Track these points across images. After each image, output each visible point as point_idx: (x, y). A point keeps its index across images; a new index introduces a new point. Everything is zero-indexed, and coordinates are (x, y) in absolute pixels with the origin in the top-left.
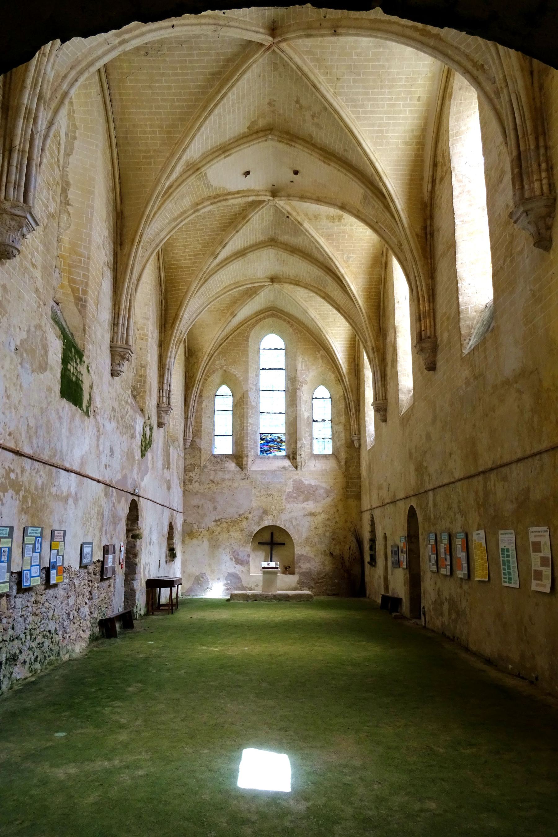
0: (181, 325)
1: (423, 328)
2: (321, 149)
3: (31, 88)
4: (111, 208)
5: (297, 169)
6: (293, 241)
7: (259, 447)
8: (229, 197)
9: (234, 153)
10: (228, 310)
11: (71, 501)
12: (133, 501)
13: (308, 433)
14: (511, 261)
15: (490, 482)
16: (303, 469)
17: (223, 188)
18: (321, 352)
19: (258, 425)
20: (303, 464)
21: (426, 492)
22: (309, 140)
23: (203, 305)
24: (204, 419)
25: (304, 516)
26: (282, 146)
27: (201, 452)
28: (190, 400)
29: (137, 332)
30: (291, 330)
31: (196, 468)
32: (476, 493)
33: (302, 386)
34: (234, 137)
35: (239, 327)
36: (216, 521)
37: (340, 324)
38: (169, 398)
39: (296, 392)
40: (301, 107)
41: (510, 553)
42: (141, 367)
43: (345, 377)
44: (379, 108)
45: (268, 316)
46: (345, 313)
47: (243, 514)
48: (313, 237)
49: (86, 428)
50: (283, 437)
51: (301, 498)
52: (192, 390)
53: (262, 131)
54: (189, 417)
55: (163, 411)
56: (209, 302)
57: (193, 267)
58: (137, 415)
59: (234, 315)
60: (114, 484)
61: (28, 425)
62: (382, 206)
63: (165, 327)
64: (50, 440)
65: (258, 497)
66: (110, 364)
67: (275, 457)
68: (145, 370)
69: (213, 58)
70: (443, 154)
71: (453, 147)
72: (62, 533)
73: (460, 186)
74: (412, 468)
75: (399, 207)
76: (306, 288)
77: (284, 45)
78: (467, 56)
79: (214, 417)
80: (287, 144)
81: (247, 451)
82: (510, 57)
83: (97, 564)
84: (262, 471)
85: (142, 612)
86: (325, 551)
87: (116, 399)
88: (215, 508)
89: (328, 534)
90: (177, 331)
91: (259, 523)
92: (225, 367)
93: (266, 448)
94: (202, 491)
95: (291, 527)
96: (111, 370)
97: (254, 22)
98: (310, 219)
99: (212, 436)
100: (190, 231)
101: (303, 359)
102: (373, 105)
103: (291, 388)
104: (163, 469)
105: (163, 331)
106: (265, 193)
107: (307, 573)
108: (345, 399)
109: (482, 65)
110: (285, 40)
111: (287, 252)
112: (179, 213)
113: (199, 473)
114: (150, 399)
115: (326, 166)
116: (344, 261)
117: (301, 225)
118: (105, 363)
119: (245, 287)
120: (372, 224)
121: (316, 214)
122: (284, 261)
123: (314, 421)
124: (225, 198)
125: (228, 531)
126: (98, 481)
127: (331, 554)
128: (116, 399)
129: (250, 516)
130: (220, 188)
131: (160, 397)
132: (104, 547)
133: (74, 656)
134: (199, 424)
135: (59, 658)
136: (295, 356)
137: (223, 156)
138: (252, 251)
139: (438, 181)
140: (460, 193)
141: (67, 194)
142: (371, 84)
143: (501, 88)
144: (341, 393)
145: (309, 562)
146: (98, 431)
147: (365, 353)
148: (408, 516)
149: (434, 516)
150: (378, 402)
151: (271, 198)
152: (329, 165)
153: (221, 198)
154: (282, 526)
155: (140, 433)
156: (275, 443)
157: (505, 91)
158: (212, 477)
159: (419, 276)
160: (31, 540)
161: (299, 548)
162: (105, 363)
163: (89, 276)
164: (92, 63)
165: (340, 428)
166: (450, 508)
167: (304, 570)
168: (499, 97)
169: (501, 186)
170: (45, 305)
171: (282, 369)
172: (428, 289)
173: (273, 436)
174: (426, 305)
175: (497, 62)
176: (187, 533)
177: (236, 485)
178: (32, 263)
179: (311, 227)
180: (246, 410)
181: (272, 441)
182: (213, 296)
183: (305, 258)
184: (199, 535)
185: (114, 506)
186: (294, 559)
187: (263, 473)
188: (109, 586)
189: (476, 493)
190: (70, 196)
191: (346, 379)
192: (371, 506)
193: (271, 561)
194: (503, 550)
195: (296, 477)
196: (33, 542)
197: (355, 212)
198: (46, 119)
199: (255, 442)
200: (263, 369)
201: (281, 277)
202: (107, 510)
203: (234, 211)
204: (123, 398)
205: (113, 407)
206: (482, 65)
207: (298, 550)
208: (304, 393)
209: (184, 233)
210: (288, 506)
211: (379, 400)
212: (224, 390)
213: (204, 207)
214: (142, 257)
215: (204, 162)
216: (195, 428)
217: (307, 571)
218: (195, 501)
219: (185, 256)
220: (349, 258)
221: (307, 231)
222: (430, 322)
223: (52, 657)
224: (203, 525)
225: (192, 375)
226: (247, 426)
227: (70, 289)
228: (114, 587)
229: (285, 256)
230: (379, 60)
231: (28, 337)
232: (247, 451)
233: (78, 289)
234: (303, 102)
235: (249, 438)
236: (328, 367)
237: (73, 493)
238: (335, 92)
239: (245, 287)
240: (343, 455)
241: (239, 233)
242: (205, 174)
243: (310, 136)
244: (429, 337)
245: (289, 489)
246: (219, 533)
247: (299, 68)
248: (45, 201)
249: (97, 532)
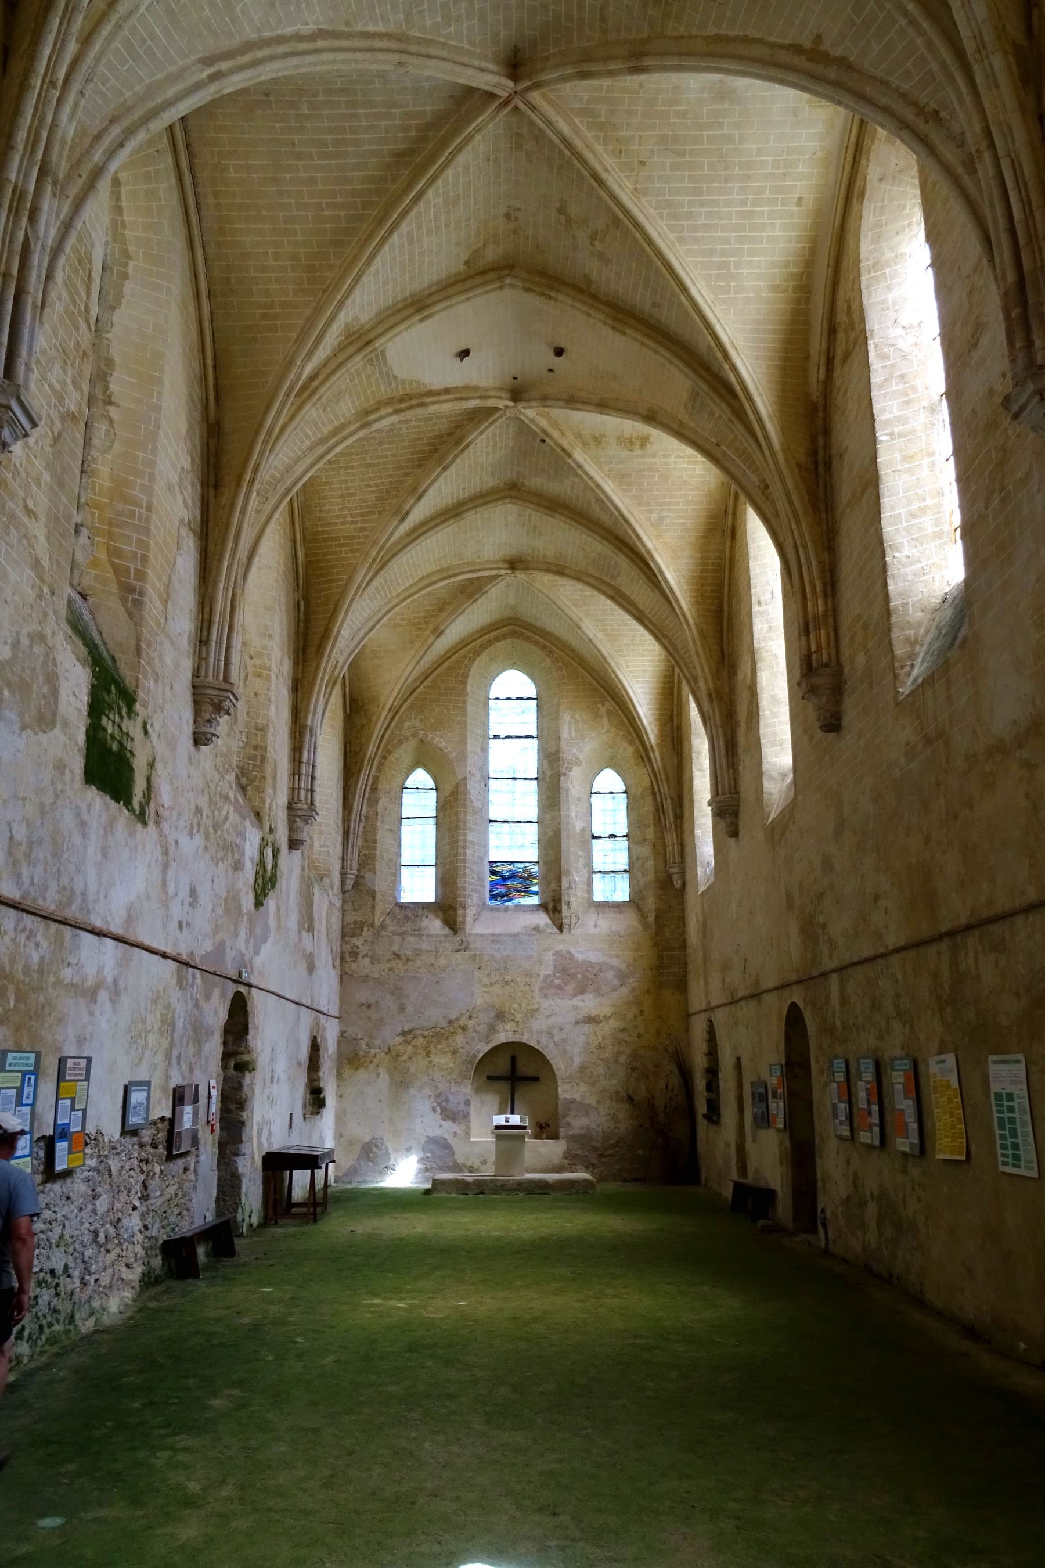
0: (336, 649)
1: (813, 648)
2: (608, 304)
3: (25, 149)
4: (197, 416)
5: (562, 346)
6: (554, 487)
7: (488, 888)
8: (428, 400)
9: (440, 311)
10: (427, 623)
11: (103, 996)
12: (238, 995)
13: (582, 861)
14: (1002, 500)
15: (966, 955)
16: (573, 931)
17: (418, 383)
18: (607, 703)
19: (485, 846)
20: (574, 921)
21: (824, 975)
22: (584, 287)
23: (378, 611)
24: (382, 835)
25: (577, 1023)
26: (532, 300)
27: (374, 898)
28: (354, 797)
29: (249, 662)
30: (548, 660)
31: (365, 929)
33: (570, 770)
34: (439, 282)
35: (449, 658)
36: (404, 1033)
37: (644, 650)
38: (312, 791)
39: (559, 780)
40: (569, 221)
41: (1014, 1104)
42: (257, 730)
43: (653, 751)
44: (721, 219)
45: (504, 636)
46: (654, 625)
47: (457, 1019)
48: (591, 478)
49: (140, 848)
50: (535, 869)
51: (570, 988)
52: (358, 780)
53: (493, 269)
54: (352, 830)
55: (299, 816)
56: (390, 606)
57: (358, 537)
58: (247, 823)
59: (438, 633)
60: (197, 961)
61: (11, 838)
62: (728, 411)
63: (304, 652)
64: (59, 870)
65: (486, 986)
66: (191, 721)
67: (519, 908)
68: (265, 736)
69: (398, 122)
70: (849, 307)
71: (869, 292)
72: (83, 1063)
73: (885, 366)
74: (794, 929)
75: (763, 411)
76: (579, 580)
77: (535, 96)
78: (904, 96)
79: (400, 829)
80: (542, 294)
81: (464, 897)
82: (998, 87)
83: (160, 1125)
84: (493, 935)
85: (255, 1220)
86: (617, 1092)
87: (203, 791)
88: (402, 1009)
89: (623, 1059)
90: (328, 661)
91: (487, 1036)
92: (422, 732)
93: (501, 890)
94: (376, 975)
95: (551, 1045)
96: (195, 733)
97: (478, 51)
98: (585, 444)
99: (395, 867)
100: (353, 467)
101: (572, 717)
102: (709, 215)
103: (548, 774)
104: (300, 932)
105: (301, 660)
106: (498, 394)
107: (583, 1136)
108: (654, 794)
109: (936, 112)
110: (537, 86)
111: (542, 509)
112: (330, 428)
113: (370, 940)
114: (275, 793)
115: (618, 336)
116: (652, 525)
117: (569, 455)
118: (180, 719)
119: (460, 578)
120: (707, 447)
121: (597, 434)
122: (535, 528)
123: (594, 837)
124: (420, 401)
125: (428, 1055)
126: (164, 956)
127: (630, 1098)
128: (203, 791)
129: (471, 1024)
130: (411, 383)
131: (293, 789)
132: (175, 1090)
133: (106, 1320)
134: (371, 843)
135: (72, 1327)
136: (558, 712)
137: (417, 317)
138: (474, 507)
139: (838, 360)
140: (885, 380)
141: (108, 382)
142: (705, 172)
143: (978, 151)
144: (646, 783)
145: (587, 1114)
146: (166, 853)
147: (693, 706)
148: (786, 1025)
149: (843, 1023)
150: (721, 798)
151: (511, 404)
152: (624, 333)
153: (414, 402)
154: (532, 1044)
155: (252, 859)
156: (519, 880)
157: (987, 156)
158: (395, 948)
159: (805, 546)
160: (14, 1080)
161: (567, 1087)
162: (180, 719)
163: (148, 544)
164: (153, 114)
165: (646, 851)
166: (876, 1006)
167: (576, 1131)
168: (972, 170)
169: (976, 355)
170: (53, 593)
171: (531, 737)
172: (822, 571)
173: (514, 867)
174: (820, 602)
175: (968, 100)
176: (348, 1059)
177: (443, 962)
178: (26, 507)
179: (589, 460)
180: (462, 815)
181: (513, 876)
182: (398, 595)
183: (576, 521)
184: (371, 1062)
185: (196, 1005)
186: (556, 1110)
187: (496, 939)
188: (186, 1169)
190: (113, 387)
191: (656, 756)
192: (709, 1003)
193: (512, 1113)
194: (998, 1096)
195: (560, 947)
196: (18, 1084)
197: (675, 426)
198: (58, 215)
199: (480, 879)
200: (496, 737)
201: (529, 559)
202: (182, 1014)
203: (439, 430)
204: (219, 789)
205: (197, 807)
206: (936, 112)
207: (565, 1092)
208: (573, 783)
209: (342, 472)
210: (545, 1004)
211: (724, 794)
212: (420, 777)
213: (381, 418)
214: (257, 512)
215: (380, 329)
216: (363, 852)
217: (584, 1132)
218: (363, 995)
219: (345, 517)
220: (661, 518)
221: (580, 466)
222: (828, 634)
223: (57, 1327)
224: (377, 1042)
225: (357, 749)
226: (464, 847)
227: (111, 570)
228: (195, 1171)
229: (535, 516)
230: (721, 125)
231: (15, 656)
232: (464, 897)
233: (128, 569)
234: (573, 211)
235: (467, 871)
236: (621, 733)
237: (110, 979)
238: (636, 189)
239: (460, 578)
240: (651, 904)
241: (447, 473)
242: (383, 352)
243: (587, 278)
244: (827, 665)
245: (547, 970)
246: (410, 1058)
247: (565, 141)
248: (58, 387)
249: (159, 1059)
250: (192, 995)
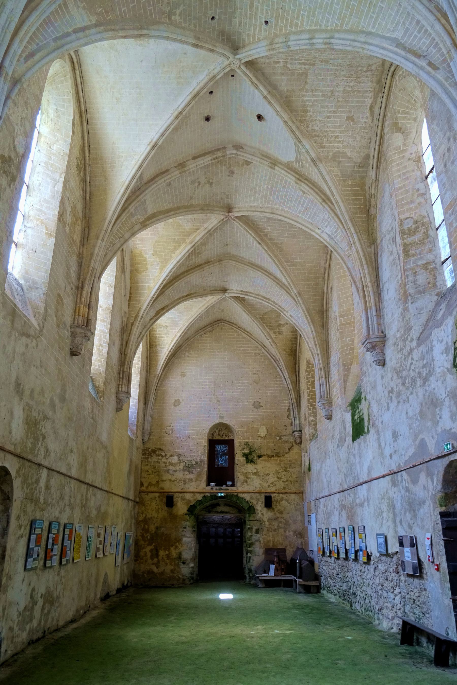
11: (366, 504)
32: (82, 495)
126: (384, 476)
149: (44, 499)
166: (62, 497)
185: (408, 490)
189: (82, 495)
202: (399, 498)
249: (390, 523)
250: (403, 487)
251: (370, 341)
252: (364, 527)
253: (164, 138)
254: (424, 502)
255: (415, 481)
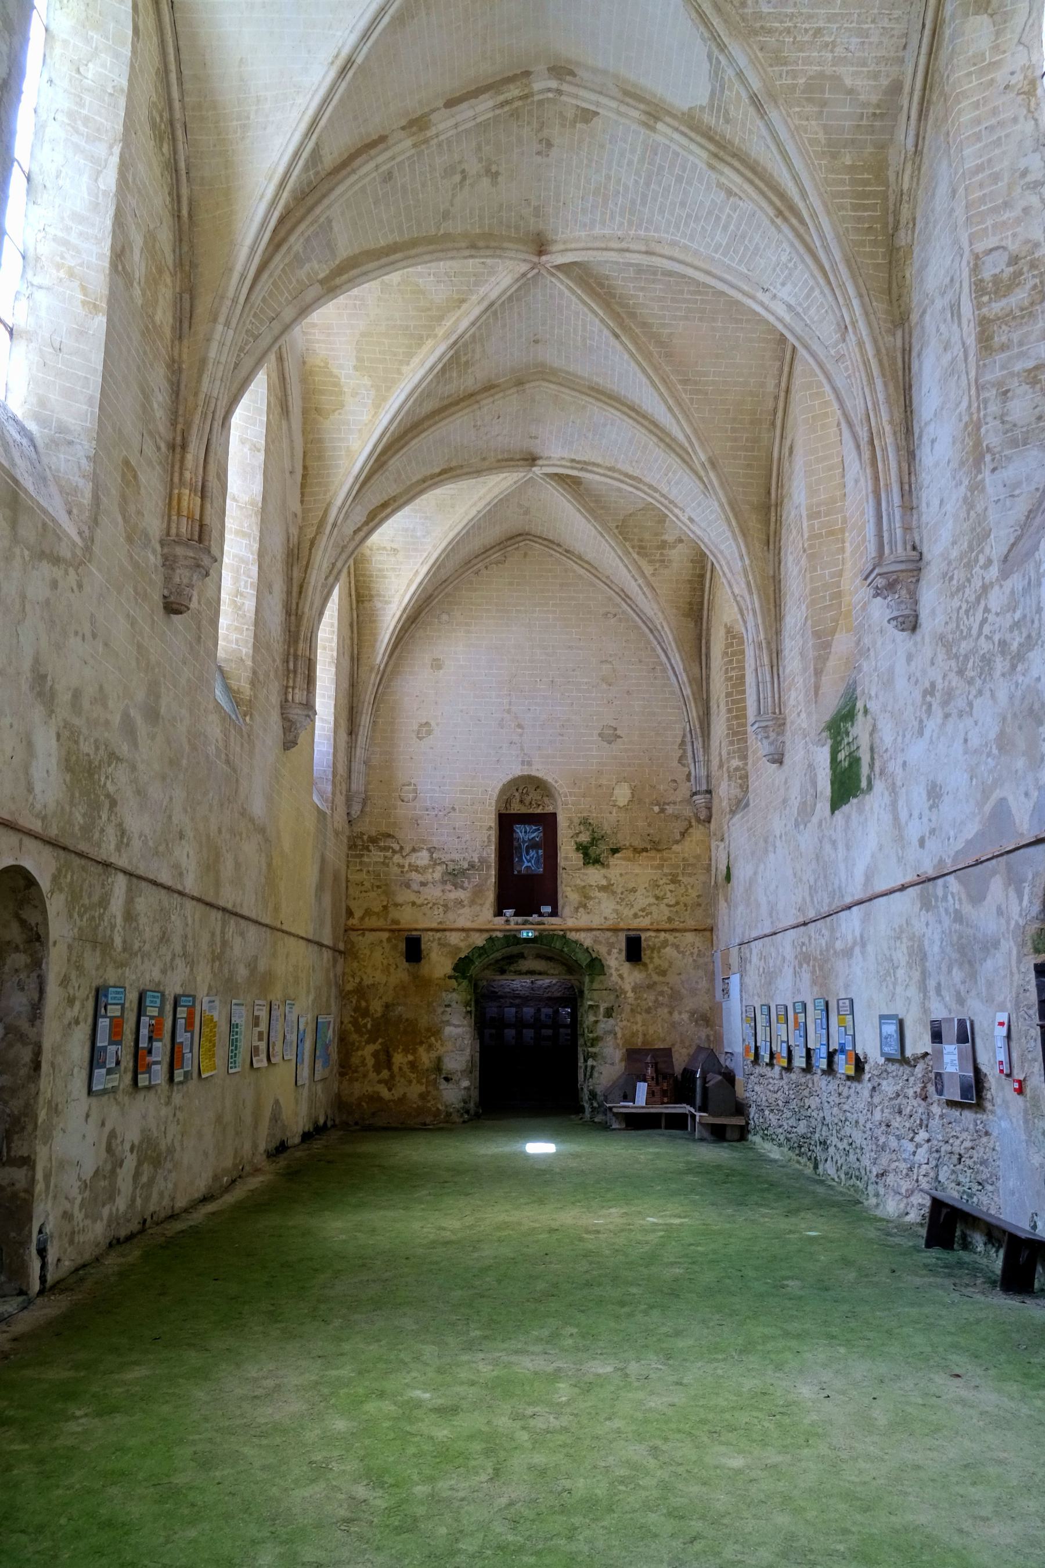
11: (857, 950)
32: (213, 934)
72: (847, 1002)
126: (903, 888)
149: (124, 942)
166: (164, 938)
185: (958, 917)
189: (213, 934)
202: (937, 937)
249: (913, 992)
250: (946, 910)
251: (884, 570)
252: (852, 1001)
253: (369, 44)
254: (996, 944)
255: (977, 898)
